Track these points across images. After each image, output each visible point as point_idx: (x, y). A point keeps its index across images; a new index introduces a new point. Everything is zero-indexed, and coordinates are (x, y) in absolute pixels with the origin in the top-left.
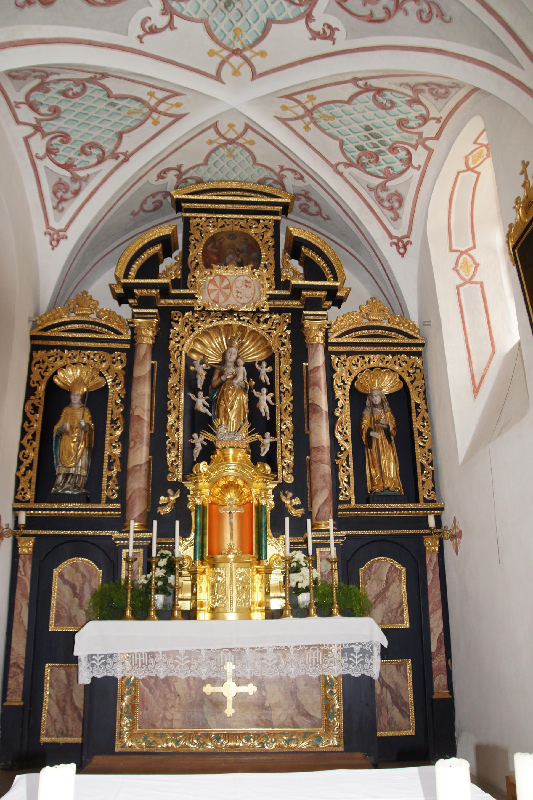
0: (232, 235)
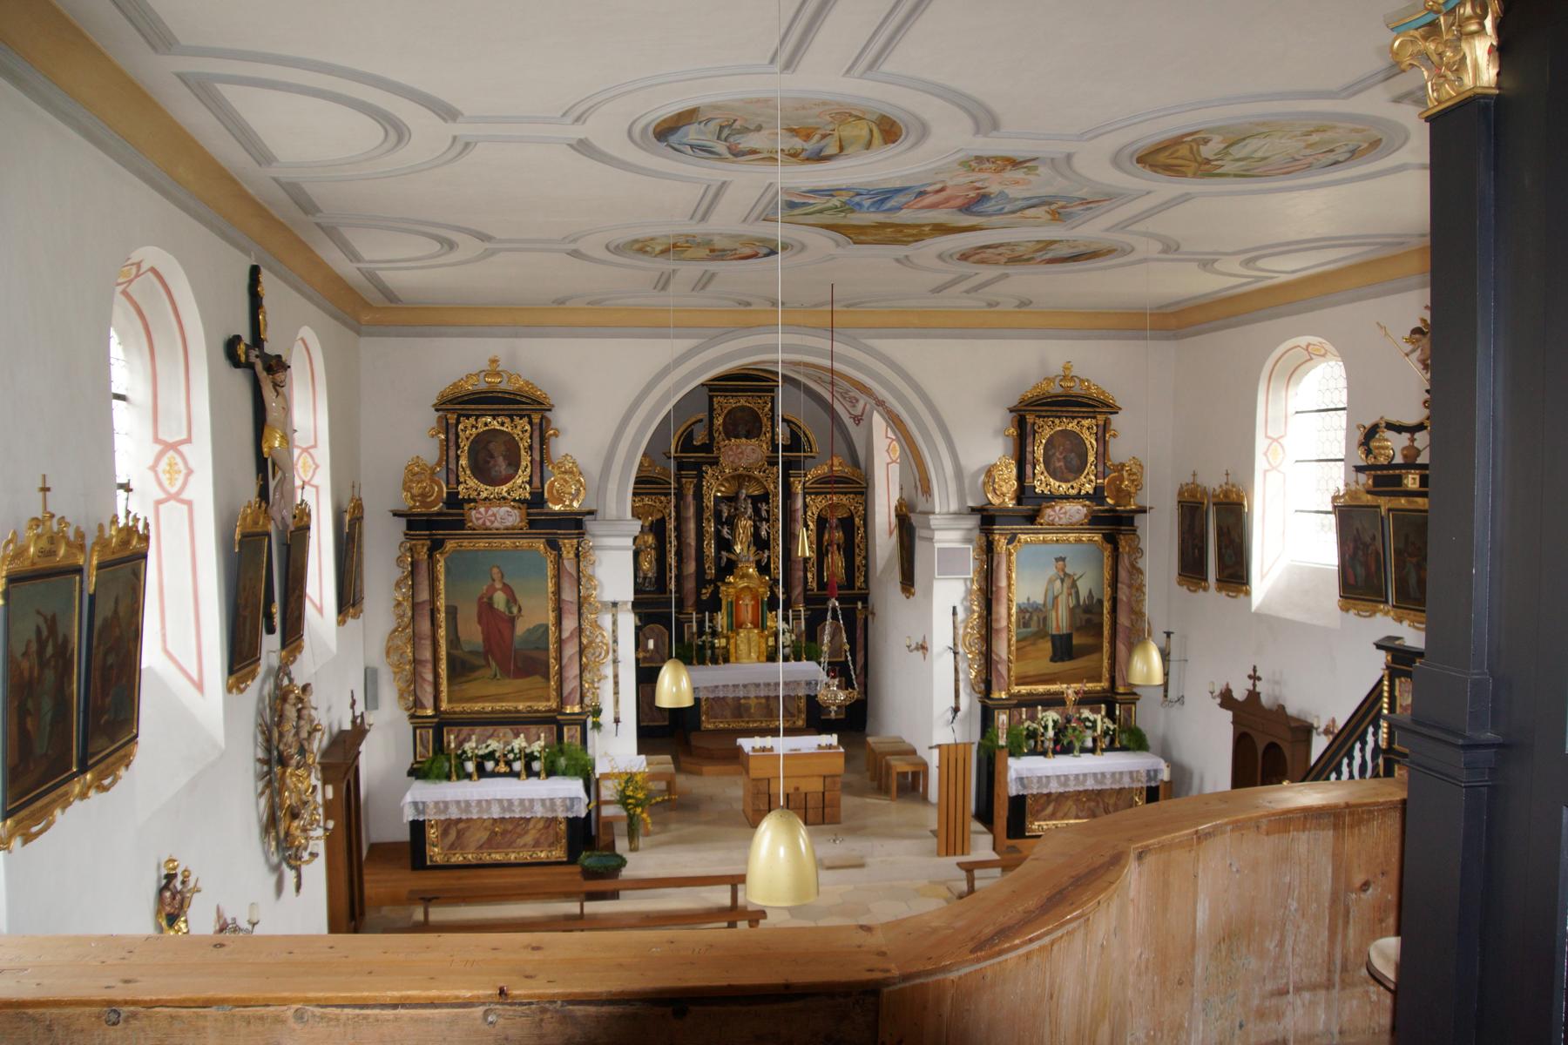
0: (743, 408)
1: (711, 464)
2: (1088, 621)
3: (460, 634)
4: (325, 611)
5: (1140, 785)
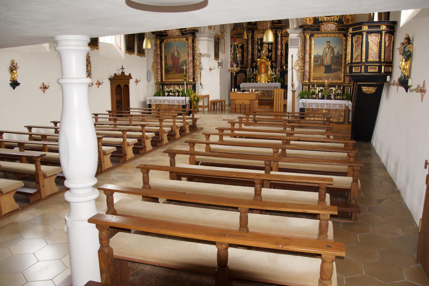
1: (257, 29)
2: (337, 61)
3: (167, 63)
4: (122, 49)
5: (342, 109)
